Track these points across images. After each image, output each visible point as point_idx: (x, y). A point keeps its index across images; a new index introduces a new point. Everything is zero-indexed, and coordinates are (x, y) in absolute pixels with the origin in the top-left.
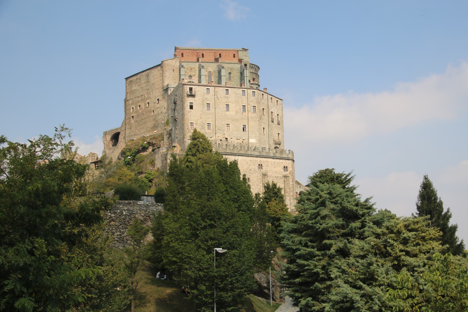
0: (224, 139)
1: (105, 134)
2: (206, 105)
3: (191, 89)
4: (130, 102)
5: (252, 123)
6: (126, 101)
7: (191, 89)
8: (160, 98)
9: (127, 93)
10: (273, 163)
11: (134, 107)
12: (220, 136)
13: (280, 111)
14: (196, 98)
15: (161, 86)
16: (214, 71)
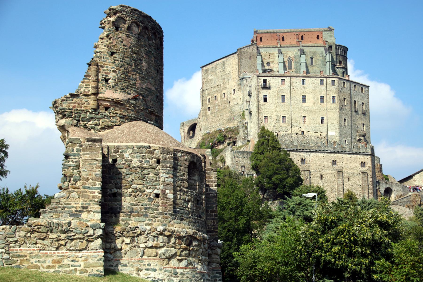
0: (300, 133)
1: (183, 125)
2: (281, 97)
3: (265, 81)
4: (206, 92)
5: (330, 115)
6: (203, 91)
7: (265, 81)
8: (237, 89)
9: (203, 83)
10: (349, 159)
11: (210, 97)
12: (296, 129)
13: (366, 99)
14: (270, 91)
15: (237, 75)
16: (295, 57)
